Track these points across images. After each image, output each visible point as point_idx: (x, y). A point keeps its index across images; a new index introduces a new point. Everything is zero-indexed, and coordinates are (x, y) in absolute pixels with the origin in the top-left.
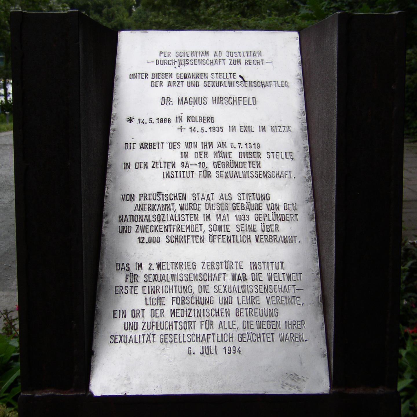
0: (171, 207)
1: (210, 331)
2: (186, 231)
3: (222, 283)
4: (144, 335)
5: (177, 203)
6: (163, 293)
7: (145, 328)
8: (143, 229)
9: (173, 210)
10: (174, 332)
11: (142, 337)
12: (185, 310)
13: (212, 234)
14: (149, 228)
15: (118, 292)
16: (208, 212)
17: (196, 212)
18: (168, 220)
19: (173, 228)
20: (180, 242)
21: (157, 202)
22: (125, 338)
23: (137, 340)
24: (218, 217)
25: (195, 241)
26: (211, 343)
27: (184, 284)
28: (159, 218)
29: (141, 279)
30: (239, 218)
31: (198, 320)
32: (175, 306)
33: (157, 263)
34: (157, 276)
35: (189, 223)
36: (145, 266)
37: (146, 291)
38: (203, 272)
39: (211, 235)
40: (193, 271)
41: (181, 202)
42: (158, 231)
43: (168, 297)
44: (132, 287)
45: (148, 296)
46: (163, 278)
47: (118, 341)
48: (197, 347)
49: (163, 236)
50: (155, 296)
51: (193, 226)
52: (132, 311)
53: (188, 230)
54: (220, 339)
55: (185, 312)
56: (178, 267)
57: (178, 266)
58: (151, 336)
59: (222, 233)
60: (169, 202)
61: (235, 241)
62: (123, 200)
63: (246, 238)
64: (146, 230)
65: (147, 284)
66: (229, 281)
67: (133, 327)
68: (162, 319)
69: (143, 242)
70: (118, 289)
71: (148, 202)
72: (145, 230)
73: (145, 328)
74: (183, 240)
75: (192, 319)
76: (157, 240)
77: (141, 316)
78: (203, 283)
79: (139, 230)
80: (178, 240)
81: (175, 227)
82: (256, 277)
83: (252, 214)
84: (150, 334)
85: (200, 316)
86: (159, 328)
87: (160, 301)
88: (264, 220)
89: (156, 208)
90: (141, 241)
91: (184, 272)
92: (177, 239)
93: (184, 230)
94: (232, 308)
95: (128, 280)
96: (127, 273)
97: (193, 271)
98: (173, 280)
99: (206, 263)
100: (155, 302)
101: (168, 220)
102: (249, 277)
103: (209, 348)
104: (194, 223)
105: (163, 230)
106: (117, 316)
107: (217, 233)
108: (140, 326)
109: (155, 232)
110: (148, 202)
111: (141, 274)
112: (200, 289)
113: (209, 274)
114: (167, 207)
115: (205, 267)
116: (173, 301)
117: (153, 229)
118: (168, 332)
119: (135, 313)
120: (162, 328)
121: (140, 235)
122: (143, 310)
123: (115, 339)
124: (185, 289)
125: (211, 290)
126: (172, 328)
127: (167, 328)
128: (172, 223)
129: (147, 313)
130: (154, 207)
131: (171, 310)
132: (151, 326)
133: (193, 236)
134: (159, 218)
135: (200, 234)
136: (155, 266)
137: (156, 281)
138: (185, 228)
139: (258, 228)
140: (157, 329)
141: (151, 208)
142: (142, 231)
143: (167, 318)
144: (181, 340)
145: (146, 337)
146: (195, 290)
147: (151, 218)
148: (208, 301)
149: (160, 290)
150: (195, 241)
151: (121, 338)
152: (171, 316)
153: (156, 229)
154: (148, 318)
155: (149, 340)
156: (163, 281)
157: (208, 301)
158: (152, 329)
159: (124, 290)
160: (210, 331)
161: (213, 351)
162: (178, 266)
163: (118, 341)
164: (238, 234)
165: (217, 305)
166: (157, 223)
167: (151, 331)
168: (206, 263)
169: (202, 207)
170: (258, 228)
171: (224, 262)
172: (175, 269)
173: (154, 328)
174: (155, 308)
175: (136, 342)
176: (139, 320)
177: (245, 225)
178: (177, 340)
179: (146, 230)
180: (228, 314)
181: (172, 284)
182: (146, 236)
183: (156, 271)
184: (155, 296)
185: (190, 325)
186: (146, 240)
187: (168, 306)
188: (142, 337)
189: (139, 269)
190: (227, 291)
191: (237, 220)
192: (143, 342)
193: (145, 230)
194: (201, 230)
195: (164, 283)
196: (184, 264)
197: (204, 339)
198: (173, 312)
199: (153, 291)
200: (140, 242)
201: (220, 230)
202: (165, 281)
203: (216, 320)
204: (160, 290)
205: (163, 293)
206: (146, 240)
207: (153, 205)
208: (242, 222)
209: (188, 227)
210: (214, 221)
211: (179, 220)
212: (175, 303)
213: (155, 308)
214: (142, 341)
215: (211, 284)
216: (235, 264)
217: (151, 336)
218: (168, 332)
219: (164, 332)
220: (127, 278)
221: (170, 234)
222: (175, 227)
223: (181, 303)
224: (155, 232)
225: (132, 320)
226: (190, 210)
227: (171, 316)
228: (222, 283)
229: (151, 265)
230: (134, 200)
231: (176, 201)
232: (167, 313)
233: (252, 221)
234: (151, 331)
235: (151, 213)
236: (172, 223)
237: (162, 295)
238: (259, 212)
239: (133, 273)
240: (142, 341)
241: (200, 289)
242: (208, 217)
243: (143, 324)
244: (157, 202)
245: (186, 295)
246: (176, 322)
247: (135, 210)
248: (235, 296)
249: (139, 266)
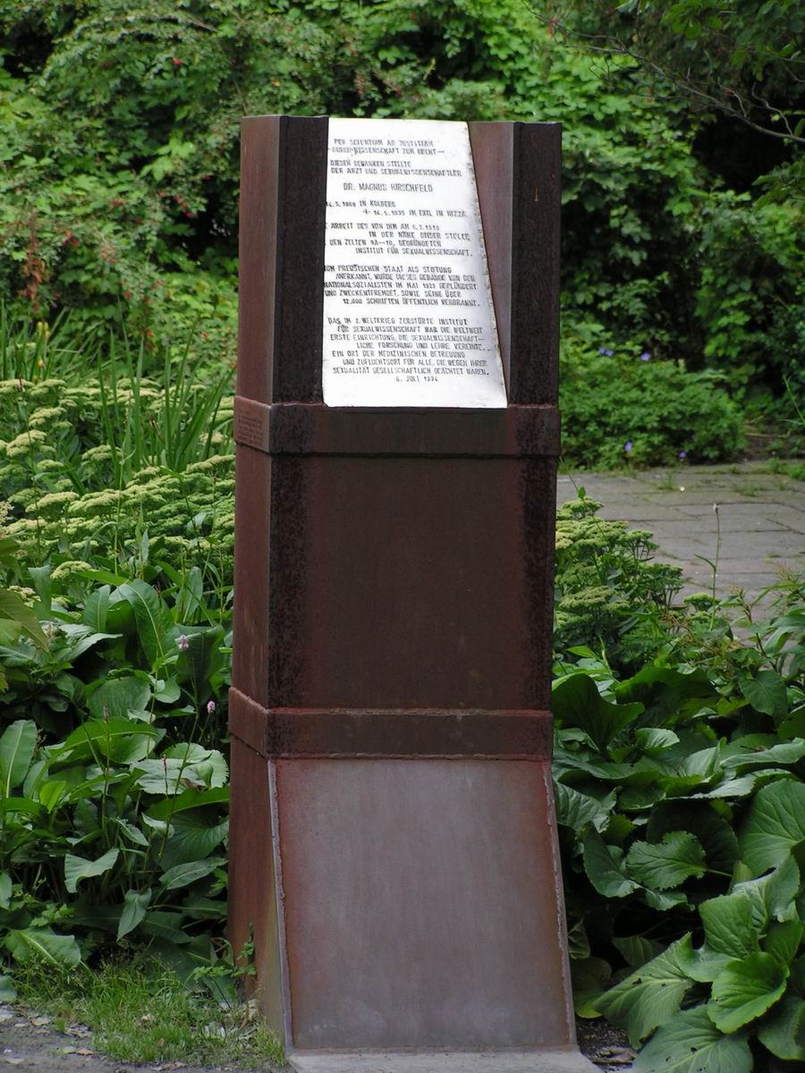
1: (412, 366)
10: (383, 366)
26: (413, 374)
27: (386, 333)
31: (402, 359)
32: (382, 349)
43: (375, 343)
46: (369, 329)
48: (403, 376)
50: (365, 341)
65: (357, 333)
66: (423, 332)
67: (351, 362)
68: (372, 358)
75: (397, 358)
78: (402, 333)
91: (386, 325)
94: (428, 350)
102: (439, 329)
103: (413, 378)
108: (356, 362)
143: (377, 356)
148: (407, 346)
157: (407, 346)
165: (415, 348)
184: (365, 341)
185: (395, 362)
187: (376, 349)
195: (369, 333)
197: (409, 371)
203: (416, 359)
215: (409, 334)
219: (376, 366)
228: (417, 333)
232: (376, 354)
248: (429, 343)
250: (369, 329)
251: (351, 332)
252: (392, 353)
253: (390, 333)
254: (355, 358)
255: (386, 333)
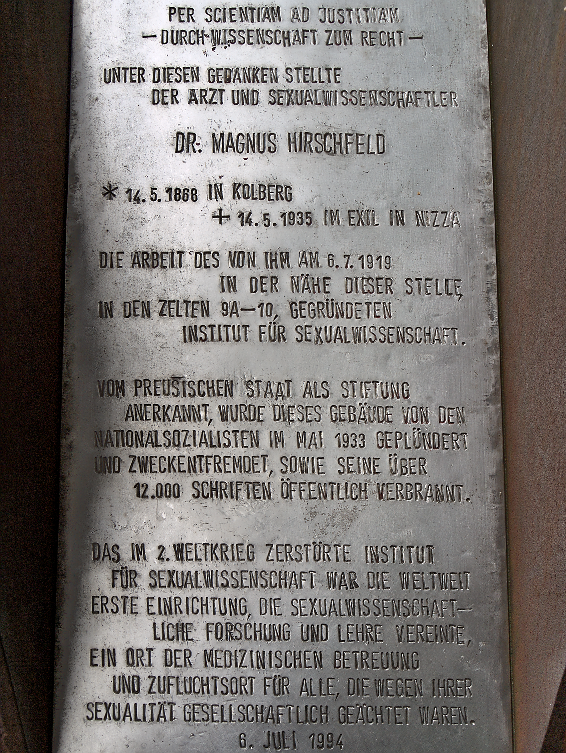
0: (202, 414)
2: (234, 472)
3: (306, 592)
4: (152, 705)
5: (215, 404)
6: (188, 613)
7: (155, 689)
8: (145, 465)
9: (206, 420)
10: (212, 700)
11: (148, 708)
12: (233, 653)
13: (288, 479)
14: (156, 461)
15: (98, 608)
16: (279, 426)
17: (254, 426)
18: (195, 445)
19: (207, 464)
20: (221, 497)
21: (172, 401)
22: (117, 710)
23: (140, 715)
24: (300, 438)
25: (251, 495)
27: (229, 594)
28: (176, 438)
29: (144, 581)
30: (344, 442)
32: (213, 644)
33: (174, 546)
34: (175, 576)
35: (240, 452)
36: (151, 551)
37: (155, 609)
38: (269, 567)
39: (285, 480)
40: (249, 566)
41: (223, 401)
42: (175, 471)
43: (199, 623)
44: (125, 598)
45: (159, 620)
46: (188, 580)
47: (101, 715)
49: (186, 482)
50: (174, 620)
51: (247, 460)
52: (127, 651)
53: (237, 470)
54: (302, 718)
55: (233, 658)
56: (219, 556)
57: (218, 553)
58: (167, 707)
59: (309, 477)
60: (197, 401)
61: (335, 496)
62: (102, 395)
63: (358, 489)
64: (151, 468)
65: (158, 593)
67: (129, 685)
68: (188, 673)
69: (144, 497)
70: (98, 601)
71: (150, 399)
72: (149, 468)
73: (155, 689)
74: (228, 491)
76: (171, 492)
77: (146, 662)
78: (270, 594)
79: (136, 467)
80: (216, 491)
81: (211, 460)
82: (377, 581)
83: (372, 431)
84: (165, 702)
85: (264, 667)
86: (182, 690)
87: (182, 630)
88: (397, 447)
89: (171, 413)
90: (141, 493)
91: (232, 567)
92: (216, 489)
93: (230, 468)
95: (118, 582)
96: (117, 567)
97: (249, 566)
98: (209, 584)
99: (274, 547)
100: (172, 633)
101: (195, 445)
102: (361, 580)
104: (252, 452)
105: (185, 467)
106: (98, 660)
107: (299, 477)
108: (145, 684)
109: (170, 471)
110: (150, 399)
111: (143, 570)
112: (263, 607)
113: (280, 572)
114: (191, 414)
115: (273, 555)
116: (208, 632)
117: (165, 465)
118: (201, 699)
119: (133, 656)
120: (188, 690)
121: (142, 478)
122: (150, 650)
123: (97, 711)
124: (234, 607)
125: (286, 609)
126: (208, 692)
127: (197, 691)
128: (206, 451)
129: (158, 658)
130: (165, 414)
131: (205, 651)
132: (163, 685)
133: (248, 483)
134: (176, 438)
135: (263, 477)
136: (170, 553)
137: (174, 586)
138: (231, 464)
139: (384, 465)
140: (178, 692)
141: (161, 414)
142: (143, 469)
143: (198, 669)
144: (226, 717)
145: (156, 709)
146: (254, 608)
147: (161, 440)
148: (278, 634)
149: (183, 607)
150: (251, 495)
151: (108, 709)
152: (206, 665)
153: (170, 464)
154: (159, 670)
155: (162, 714)
156: (189, 586)
158: (169, 692)
159: (110, 606)
160: (285, 699)
161: (289, 743)
162: (218, 553)
163: (101, 715)
164: (342, 480)
166: (172, 452)
167: (167, 698)
168: (274, 547)
169: (267, 414)
170: (384, 465)
171: (312, 546)
172: (212, 559)
173: (173, 689)
174: (174, 645)
175: (137, 719)
176: (143, 673)
177: (356, 459)
178: (217, 717)
179: (151, 468)
180: (319, 663)
181: (205, 593)
182: (152, 480)
183: (173, 565)
184: (174, 620)
186: (151, 491)
187: (200, 641)
188: (148, 708)
189: (138, 559)
190: (318, 612)
191: (340, 446)
192: (152, 719)
193: (149, 468)
194: (265, 471)
195: (189, 592)
196: (230, 548)
198: (209, 657)
199: (168, 608)
200: (138, 495)
201: (304, 470)
202: (192, 587)
204: (183, 607)
205: (188, 613)
206: (151, 491)
207: (164, 406)
208: (350, 452)
209: (238, 462)
210: (290, 446)
211: (220, 446)
212: (212, 636)
213: (174, 645)
214: (148, 718)
216: (333, 549)
217: (167, 707)
218: (201, 699)
219: (192, 699)
220: (114, 579)
221: (201, 478)
222: (211, 460)
223: (224, 637)
224: (170, 471)
225: (128, 672)
226: (241, 420)
227: (206, 665)
228: (306, 592)
229: (162, 548)
230: (123, 395)
231: (213, 398)
232: (197, 659)
233: (371, 450)
234: (167, 698)
235: (159, 427)
236: (206, 451)
237: (186, 619)
238: (385, 427)
239: (126, 567)
240: (148, 718)
241: (263, 607)
242: (277, 439)
243: (150, 681)
244: (172, 401)
245: (234, 620)
246: (215, 678)
247: (126, 420)
248: (333, 622)
249: (139, 551)
250: (188, 580)
251: (143, 591)
252: (234, 660)
253: (238, 594)
254: (143, 673)
255: (229, 594)
